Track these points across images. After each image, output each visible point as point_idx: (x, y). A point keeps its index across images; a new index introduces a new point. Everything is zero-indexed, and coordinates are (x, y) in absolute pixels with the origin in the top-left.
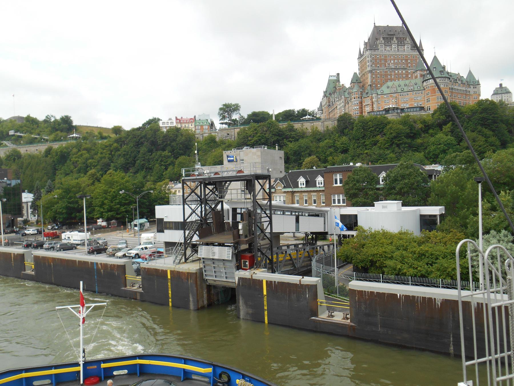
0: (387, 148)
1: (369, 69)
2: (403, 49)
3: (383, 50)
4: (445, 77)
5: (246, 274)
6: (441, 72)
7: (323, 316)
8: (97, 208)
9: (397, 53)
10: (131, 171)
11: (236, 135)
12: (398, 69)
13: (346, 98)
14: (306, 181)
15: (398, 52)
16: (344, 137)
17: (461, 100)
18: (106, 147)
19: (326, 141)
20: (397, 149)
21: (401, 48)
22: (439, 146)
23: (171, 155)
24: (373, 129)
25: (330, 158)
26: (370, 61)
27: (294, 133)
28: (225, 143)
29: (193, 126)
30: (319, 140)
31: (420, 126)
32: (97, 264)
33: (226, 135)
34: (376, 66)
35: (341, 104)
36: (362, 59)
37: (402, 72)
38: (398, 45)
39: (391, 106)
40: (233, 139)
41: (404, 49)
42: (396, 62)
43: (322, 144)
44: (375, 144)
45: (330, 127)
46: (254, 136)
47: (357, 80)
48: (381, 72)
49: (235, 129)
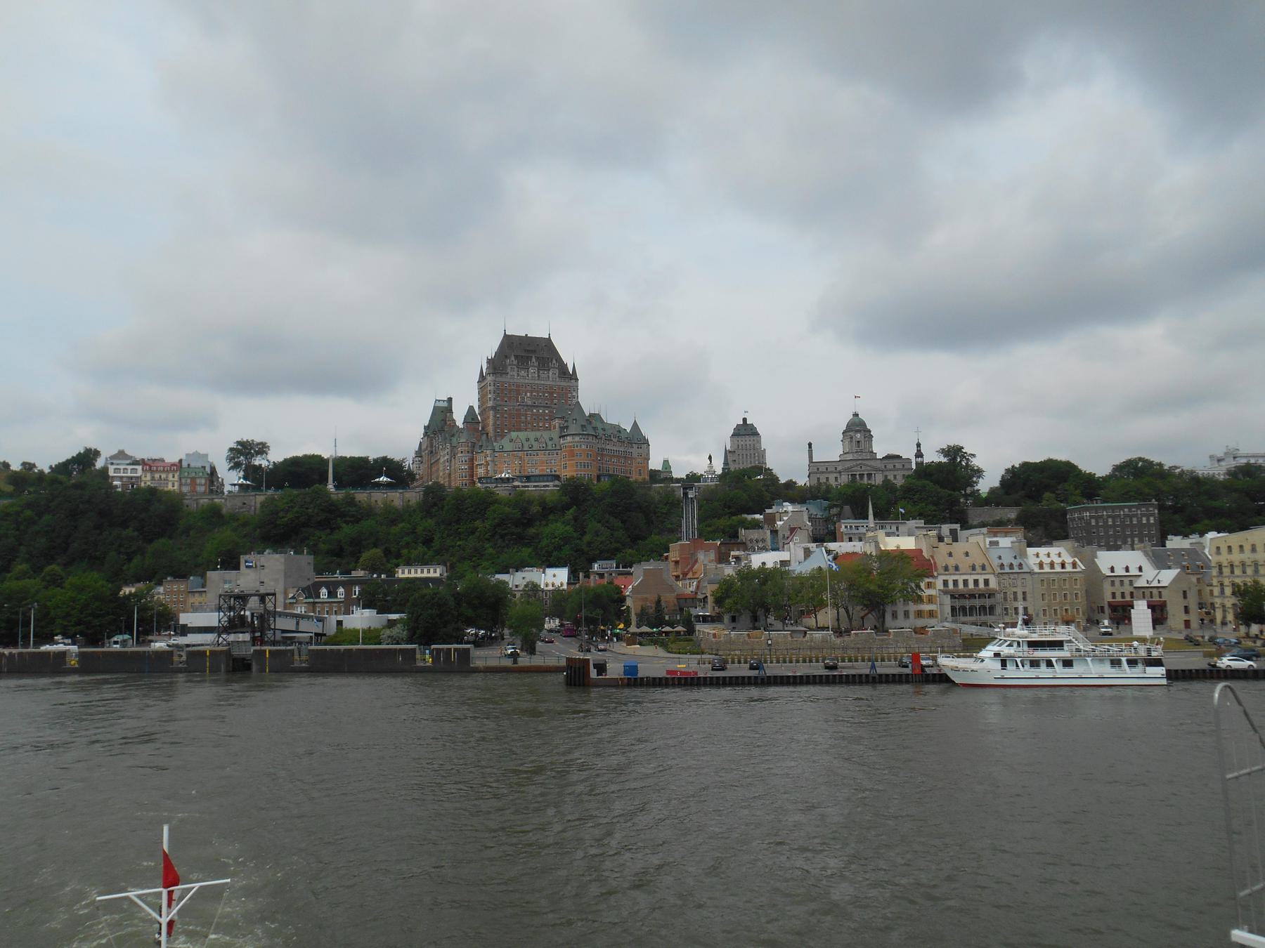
0: (488, 540)
1: (490, 404)
2: (546, 376)
3: (515, 376)
4: (588, 435)
5: (258, 648)
6: (583, 426)
7: (296, 665)
8: (59, 621)
9: (536, 382)
10: (59, 560)
11: (258, 506)
12: (537, 406)
13: (453, 448)
14: (328, 592)
15: (538, 379)
16: (429, 521)
17: (617, 466)
18: (8, 515)
19: (401, 525)
20: (500, 541)
21: (543, 374)
22: (553, 541)
23: (138, 536)
24: (472, 509)
25: (405, 552)
26: (492, 392)
27: (354, 509)
28: (238, 519)
29: (176, 478)
30: (393, 522)
31: (535, 509)
32: (148, 652)
33: (241, 505)
34: (502, 400)
35: (444, 456)
36: (483, 385)
37: (544, 411)
38: (538, 369)
39: (503, 475)
40: (252, 513)
41: (548, 376)
42: (535, 396)
43: (395, 530)
44: (473, 533)
45: (413, 502)
46: (287, 511)
47: (473, 419)
48: (510, 410)
49: (257, 496)
